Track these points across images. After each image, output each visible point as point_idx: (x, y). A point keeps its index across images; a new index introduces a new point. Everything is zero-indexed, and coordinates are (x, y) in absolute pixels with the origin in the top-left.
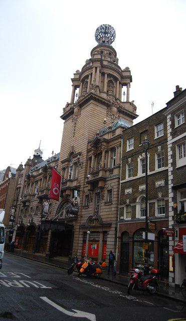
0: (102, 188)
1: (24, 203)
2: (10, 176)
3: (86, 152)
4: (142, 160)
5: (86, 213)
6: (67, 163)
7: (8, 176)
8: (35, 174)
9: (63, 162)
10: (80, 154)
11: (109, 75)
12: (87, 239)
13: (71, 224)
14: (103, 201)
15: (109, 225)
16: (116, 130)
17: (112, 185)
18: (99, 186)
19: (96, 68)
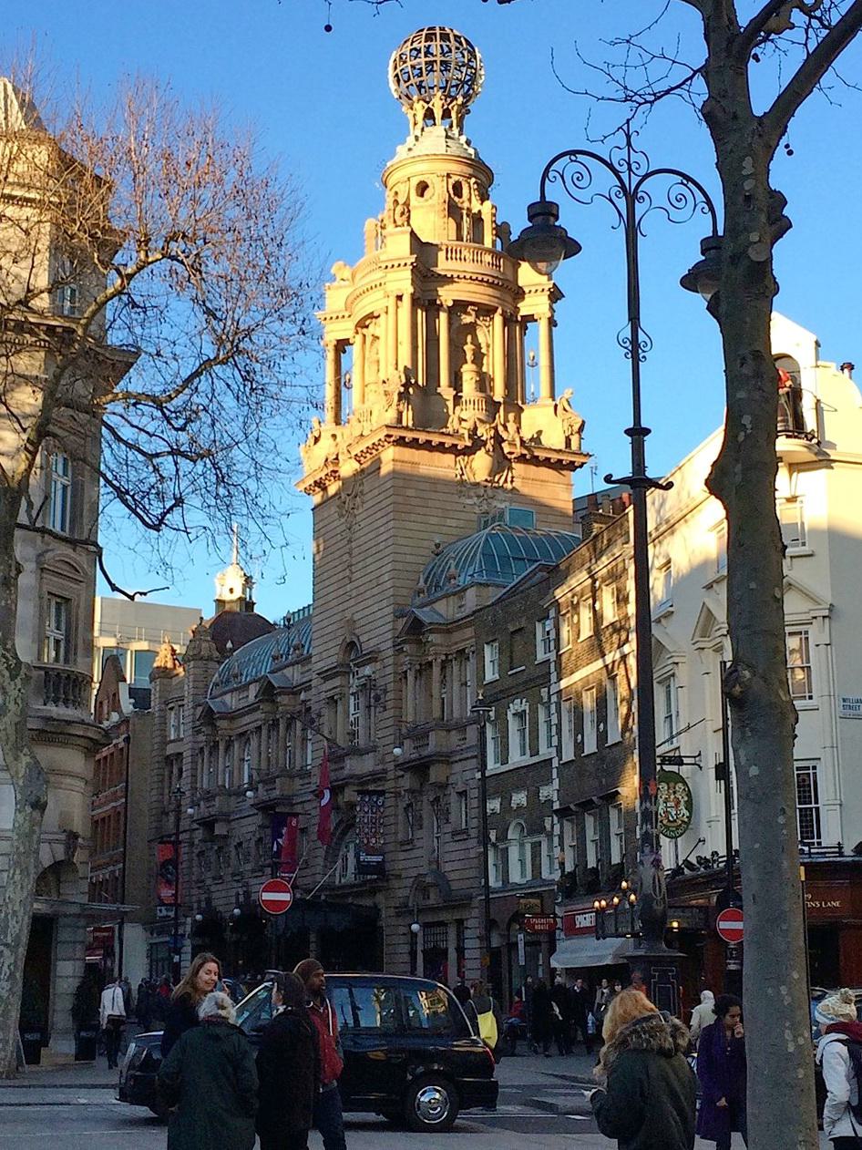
0: (443, 786)
1: (208, 824)
2: (127, 705)
3: (390, 652)
4: (520, 715)
5: (409, 864)
6: (337, 682)
7: (116, 706)
8: (232, 701)
9: (327, 675)
10: (372, 658)
11: (459, 306)
12: (420, 948)
13: (367, 902)
14: (448, 828)
15: (463, 903)
16: (464, 590)
17: (468, 775)
18: (432, 779)
19: (399, 298)
